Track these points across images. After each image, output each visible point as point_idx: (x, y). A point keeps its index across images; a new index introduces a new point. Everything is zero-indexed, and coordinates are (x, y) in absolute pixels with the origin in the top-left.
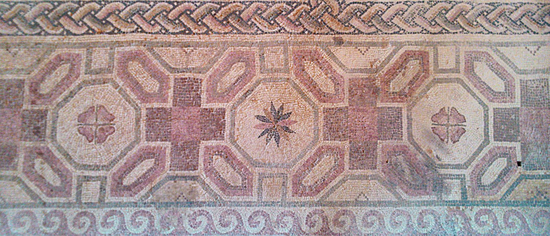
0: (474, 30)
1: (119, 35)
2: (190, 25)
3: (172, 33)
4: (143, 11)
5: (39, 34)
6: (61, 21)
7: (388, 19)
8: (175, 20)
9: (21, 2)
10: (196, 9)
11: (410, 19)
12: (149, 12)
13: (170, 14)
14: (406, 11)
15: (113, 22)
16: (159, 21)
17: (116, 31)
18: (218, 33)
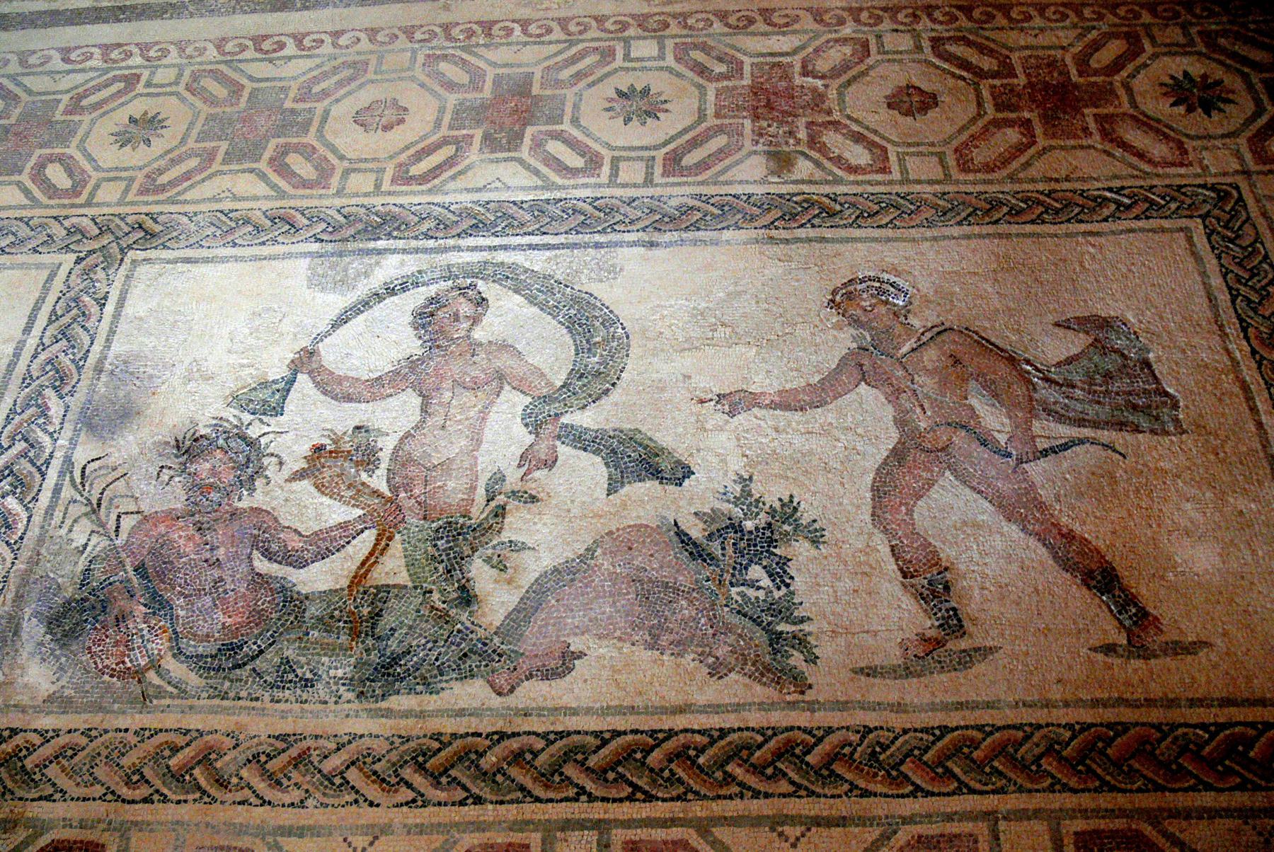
0: (229, 797)
7: (37, 766)
11: (88, 766)
14: (84, 748)
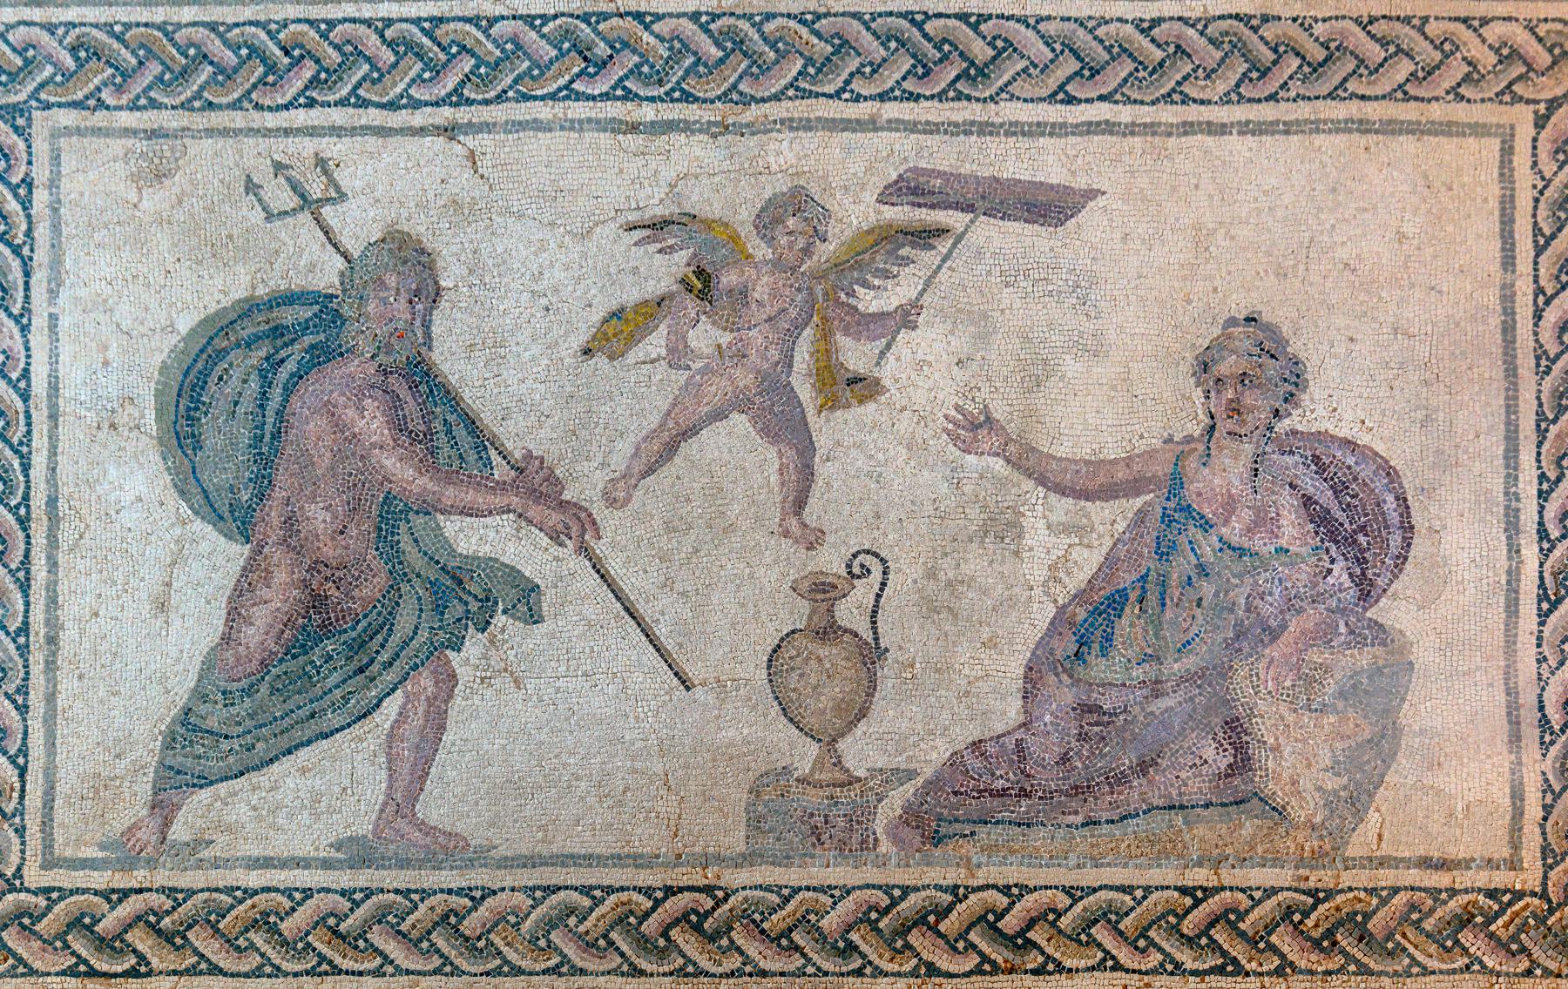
1: (1057, 976)
2: (1238, 950)
3: (1194, 973)
4: (1117, 914)
6: (914, 938)
8: (1199, 937)
9: (808, 889)
10: (1253, 907)
12: (1133, 915)
13: (1186, 922)
15: (1043, 943)
16: (1157, 940)
17: (1051, 967)
18: (1311, 972)
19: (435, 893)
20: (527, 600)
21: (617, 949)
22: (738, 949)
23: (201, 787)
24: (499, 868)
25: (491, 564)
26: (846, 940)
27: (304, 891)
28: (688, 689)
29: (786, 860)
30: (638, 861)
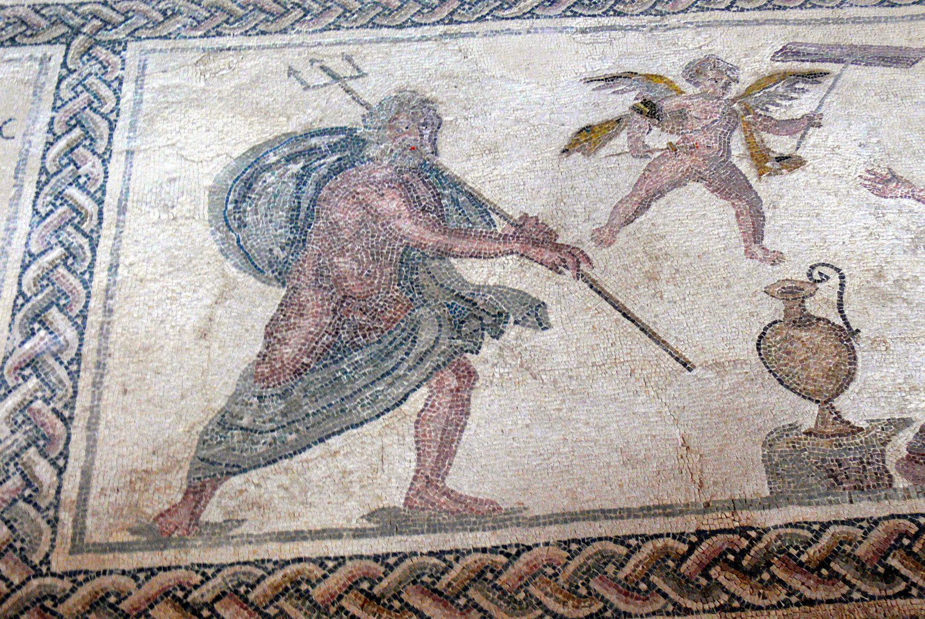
5: (905, 594)
19: (469, 552)
20: (535, 314)
21: (659, 591)
22: (782, 583)
23: (235, 474)
24: (531, 526)
25: (500, 291)
26: (884, 566)
27: (336, 559)
28: (690, 370)
29: (807, 500)
30: (667, 511)
